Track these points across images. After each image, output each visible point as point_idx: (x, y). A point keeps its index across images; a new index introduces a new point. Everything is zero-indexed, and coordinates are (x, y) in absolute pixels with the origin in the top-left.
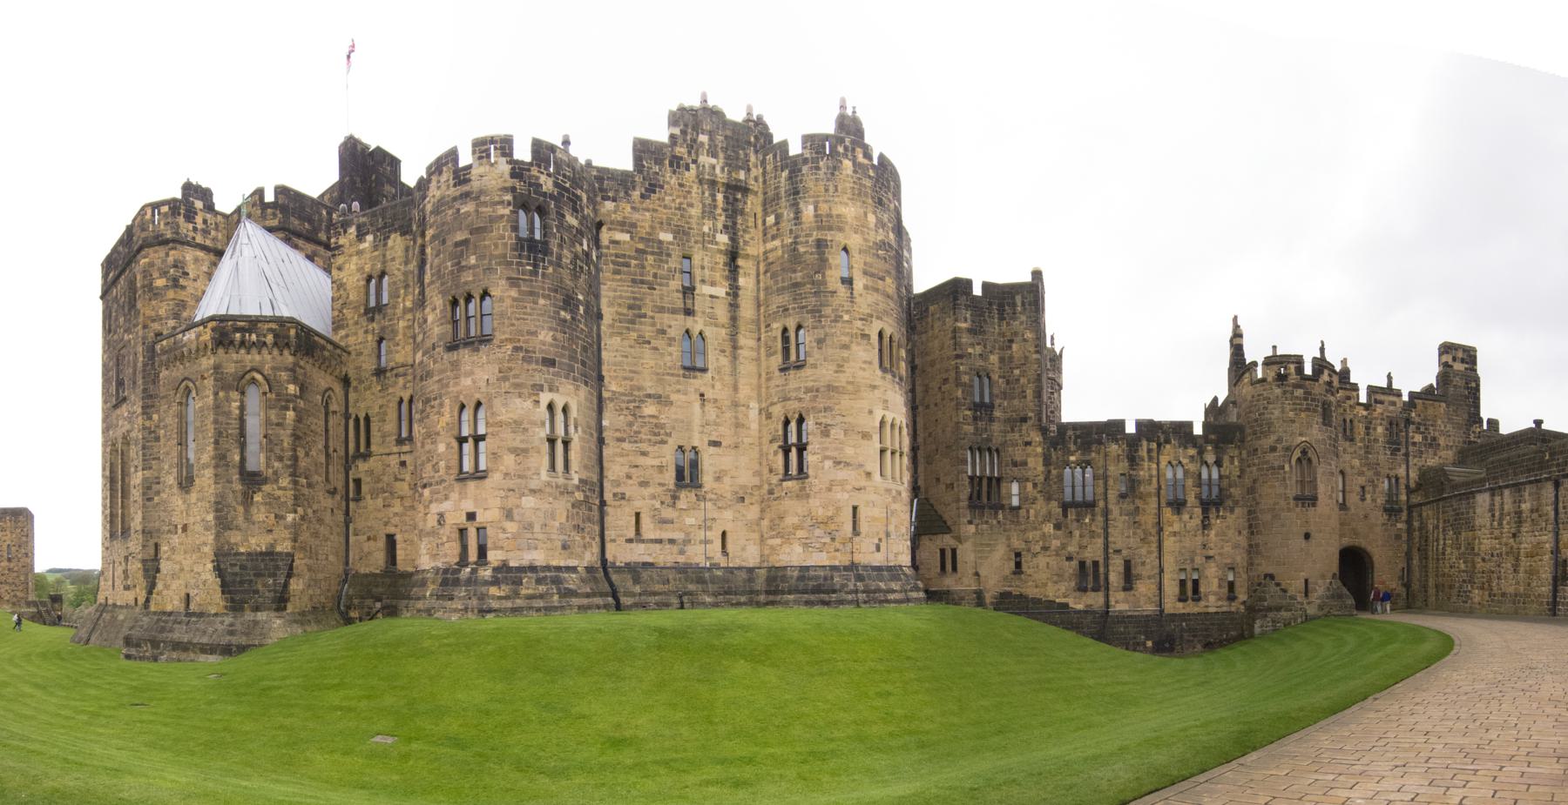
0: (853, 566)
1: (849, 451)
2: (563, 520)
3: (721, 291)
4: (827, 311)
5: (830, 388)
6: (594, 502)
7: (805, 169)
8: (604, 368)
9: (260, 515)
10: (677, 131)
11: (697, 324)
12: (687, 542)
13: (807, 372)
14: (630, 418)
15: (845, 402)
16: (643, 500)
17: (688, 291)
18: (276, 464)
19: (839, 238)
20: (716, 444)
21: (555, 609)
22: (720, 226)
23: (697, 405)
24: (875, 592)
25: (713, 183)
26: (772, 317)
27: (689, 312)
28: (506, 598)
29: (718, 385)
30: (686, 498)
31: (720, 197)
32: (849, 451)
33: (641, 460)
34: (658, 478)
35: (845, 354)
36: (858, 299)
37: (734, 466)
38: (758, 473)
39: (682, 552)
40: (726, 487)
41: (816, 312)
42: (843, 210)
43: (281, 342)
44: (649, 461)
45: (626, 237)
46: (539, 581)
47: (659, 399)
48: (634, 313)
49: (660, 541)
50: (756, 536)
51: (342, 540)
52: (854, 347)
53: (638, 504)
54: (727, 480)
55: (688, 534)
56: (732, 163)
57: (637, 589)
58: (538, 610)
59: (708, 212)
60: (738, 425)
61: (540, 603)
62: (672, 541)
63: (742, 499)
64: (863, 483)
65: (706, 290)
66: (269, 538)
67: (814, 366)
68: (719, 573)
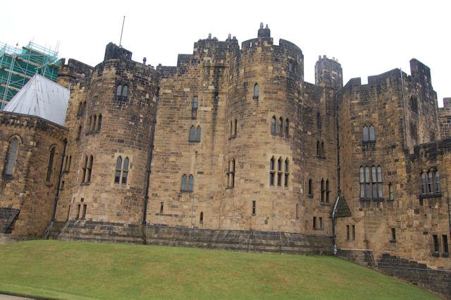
0: (251, 231)
1: (252, 174)
2: (119, 204)
3: (209, 109)
4: (246, 112)
5: (245, 145)
6: (142, 196)
7: (242, 55)
8: (155, 142)
9: (8, 192)
10: (196, 50)
11: (197, 123)
12: (183, 216)
13: (237, 139)
14: (163, 162)
15: (251, 152)
16: (165, 197)
17: (194, 110)
18: (19, 172)
19: (254, 80)
20: (201, 173)
21: (105, 240)
22: (211, 83)
23: (194, 157)
24: (259, 245)
25: (209, 67)
26: (228, 117)
27: (193, 118)
28: (87, 234)
29: (204, 148)
30: (185, 197)
31: (212, 72)
32: (252, 174)
33: (166, 180)
34: (173, 188)
35: (253, 129)
36: (260, 105)
37: (208, 183)
38: (220, 186)
39: (180, 221)
40: (205, 192)
41: (242, 113)
42: (256, 68)
43: (30, 125)
44: (169, 180)
45: (170, 91)
46: (101, 228)
47: (177, 155)
48: (171, 119)
49: (171, 215)
50: (218, 215)
51: (53, 206)
52: (257, 126)
53: (162, 199)
54: (205, 189)
55: (184, 213)
56: (217, 58)
57: (156, 236)
58: (98, 240)
59: (206, 78)
60: (213, 164)
61: (99, 237)
62: (176, 216)
63: (212, 198)
64: (258, 190)
65: (203, 109)
66: (11, 202)
67: (239, 137)
68: (197, 231)
